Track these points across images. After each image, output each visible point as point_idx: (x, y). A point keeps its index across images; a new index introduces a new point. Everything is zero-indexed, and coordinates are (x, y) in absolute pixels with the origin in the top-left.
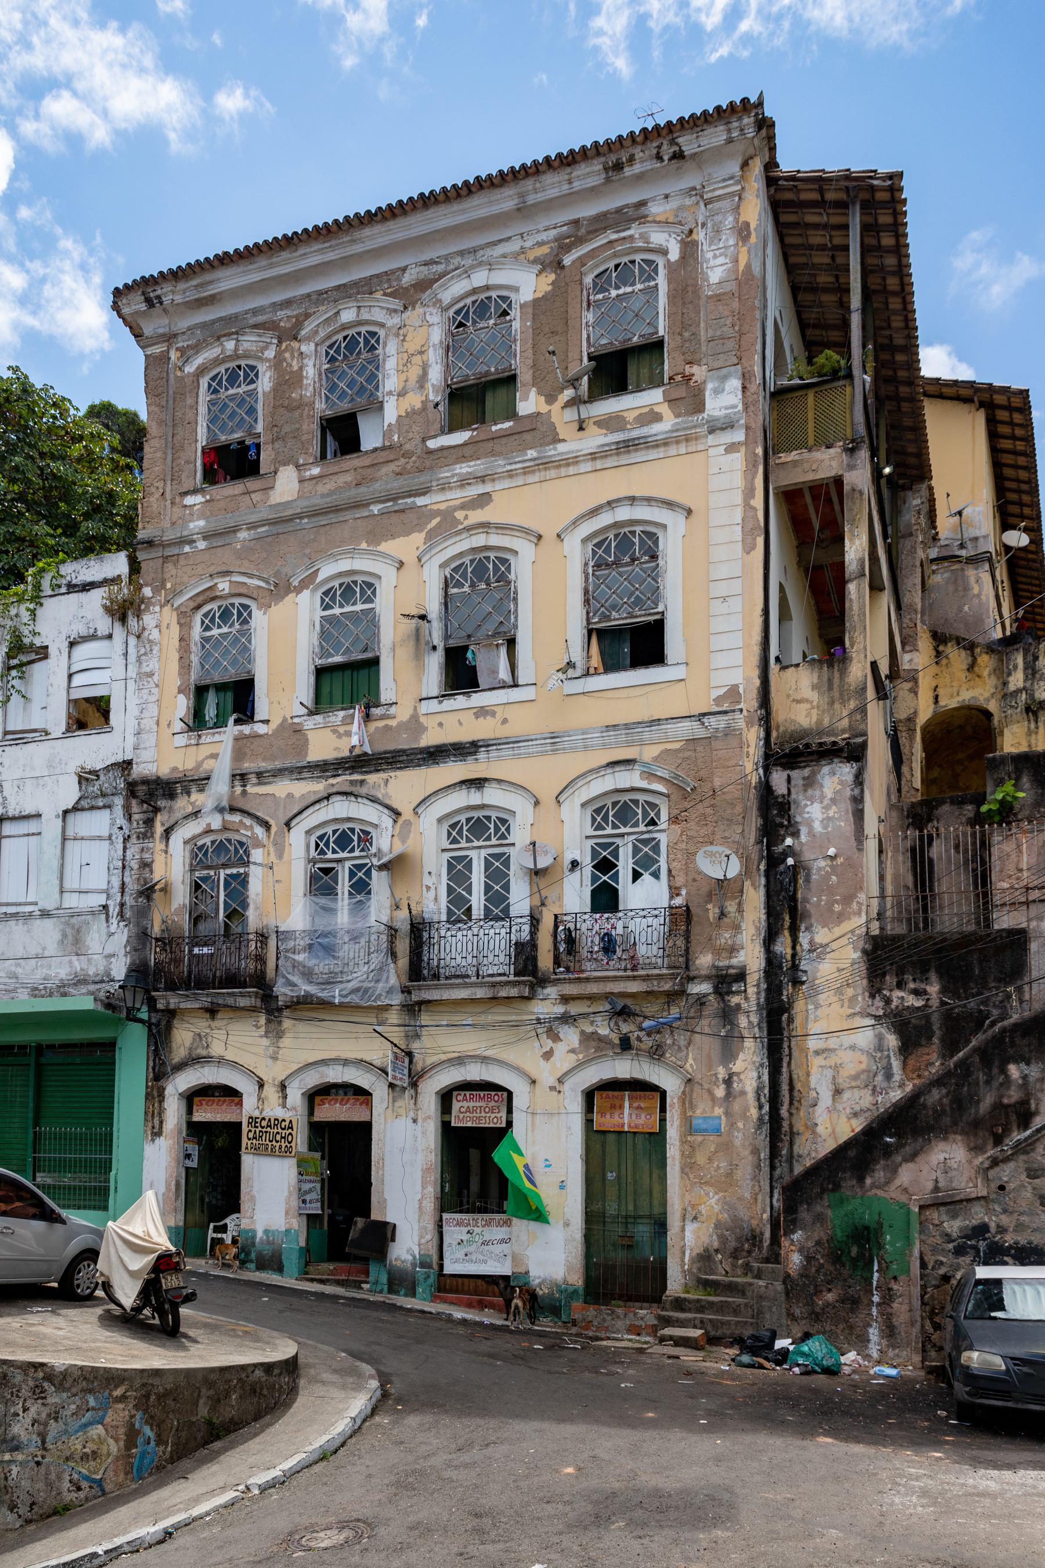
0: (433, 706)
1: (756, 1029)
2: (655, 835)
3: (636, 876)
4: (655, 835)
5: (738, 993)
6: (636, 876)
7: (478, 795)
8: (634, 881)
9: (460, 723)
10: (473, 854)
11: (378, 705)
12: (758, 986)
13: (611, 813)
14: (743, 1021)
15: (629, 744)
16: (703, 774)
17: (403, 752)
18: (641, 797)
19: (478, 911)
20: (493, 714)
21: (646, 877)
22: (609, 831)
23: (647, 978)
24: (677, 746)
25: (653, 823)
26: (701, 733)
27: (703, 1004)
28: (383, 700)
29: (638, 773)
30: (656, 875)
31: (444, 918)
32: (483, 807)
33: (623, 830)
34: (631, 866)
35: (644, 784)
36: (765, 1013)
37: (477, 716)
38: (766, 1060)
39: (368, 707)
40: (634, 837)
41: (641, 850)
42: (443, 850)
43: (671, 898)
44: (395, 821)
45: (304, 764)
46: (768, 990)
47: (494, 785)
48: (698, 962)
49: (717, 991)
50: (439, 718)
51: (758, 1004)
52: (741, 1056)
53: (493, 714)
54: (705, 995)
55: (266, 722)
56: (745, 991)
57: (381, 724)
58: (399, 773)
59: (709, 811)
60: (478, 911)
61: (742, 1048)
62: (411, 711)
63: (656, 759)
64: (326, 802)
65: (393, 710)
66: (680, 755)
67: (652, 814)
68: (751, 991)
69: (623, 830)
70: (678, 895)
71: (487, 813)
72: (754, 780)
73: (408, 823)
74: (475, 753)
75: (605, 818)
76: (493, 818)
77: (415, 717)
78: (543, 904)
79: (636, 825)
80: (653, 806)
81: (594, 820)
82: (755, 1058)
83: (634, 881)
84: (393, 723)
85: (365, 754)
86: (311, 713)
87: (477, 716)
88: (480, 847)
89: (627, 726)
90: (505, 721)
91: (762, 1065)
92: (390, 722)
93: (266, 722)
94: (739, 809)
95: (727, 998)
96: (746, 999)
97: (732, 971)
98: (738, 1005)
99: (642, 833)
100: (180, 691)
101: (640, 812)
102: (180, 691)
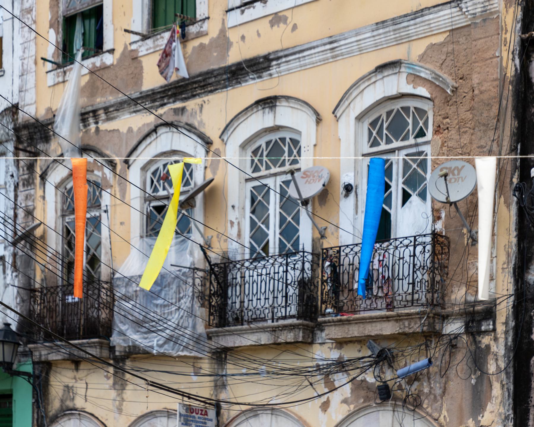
0: (235, 18)
1: (503, 376)
2: (421, 148)
3: (406, 197)
4: (421, 148)
5: (486, 332)
6: (406, 197)
7: (271, 115)
8: (404, 202)
9: (259, 35)
10: (270, 182)
11: (194, 22)
12: (506, 323)
13: (385, 125)
14: (492, 368)
15: (399, 42)
16: (463, 71)
17: (210, 73)
18: (411, 104)
19: (274, 249)
20: (284, 20)
21: (414, 199)
22: (383, 147)
23: (398, 318)
24: (440, 39)
25: (421, 134)
26: (462, 21)
27: (454, 346)
28: (198, 17)
29: (404, 76)
30: (423, 196)
31: (247, 257)
32: (277, 128)
33: (396, 144)
34: (401, 186)
35: (408, 89)
36: (512, 355)
37: (272, 24)
38: (511, 412)
39: (183, 26)
40: (405, 152)
41: (411, 166)
42: (247, 180)
43: (434, 221)
44: (207, 152)
45: (137, 95)
46: (516, 329)
47: (284, 103)
48: (453, 297)
49: (468, 331)
50: (242, 31)
51: (506, 345)
52: (489, 407)
53: (284, 20)
54: (457, 336)
55: (112, 51)
56: (494, 330)
57: (195, 43)
58: (211, 97)
59: (469, 115)
60: (274, 249)
61: (490, 398)
62: (220, 26)
63: (422, 57)
64: (154, 136)
65: (206, 26)
66: (445, 50)
67: (421, 124)
68: (500, 328)
69: (396, 144)
70: (439, 218)
71: (281, 134)
72: (510, 72)
73: (217, 154)
74: (268, 68)
75: (380, 132)
76: (288, 140)
77: (223, 32)
78: (323, 236)
79: (405, 138)
80: (421, 112)
81: (370, 134)
82: (502, 410)
83: (404, 202)
84: (205, 40)
85: (184, 79)
86: (145, 38)
87: (272, 24)
88: (275, 175)
89: (395, 21)
90: (295, 27)
91: (507, 418)
92: (205, 40)
93: (112, 51)
94: (495, 110)
95: (478, 338)
96: (496, 339)
97: (479, 308)
98: (488, 347)
99: (411, 146)
100: (50, 27)
101: (410, 121)
102: (50, 27)
